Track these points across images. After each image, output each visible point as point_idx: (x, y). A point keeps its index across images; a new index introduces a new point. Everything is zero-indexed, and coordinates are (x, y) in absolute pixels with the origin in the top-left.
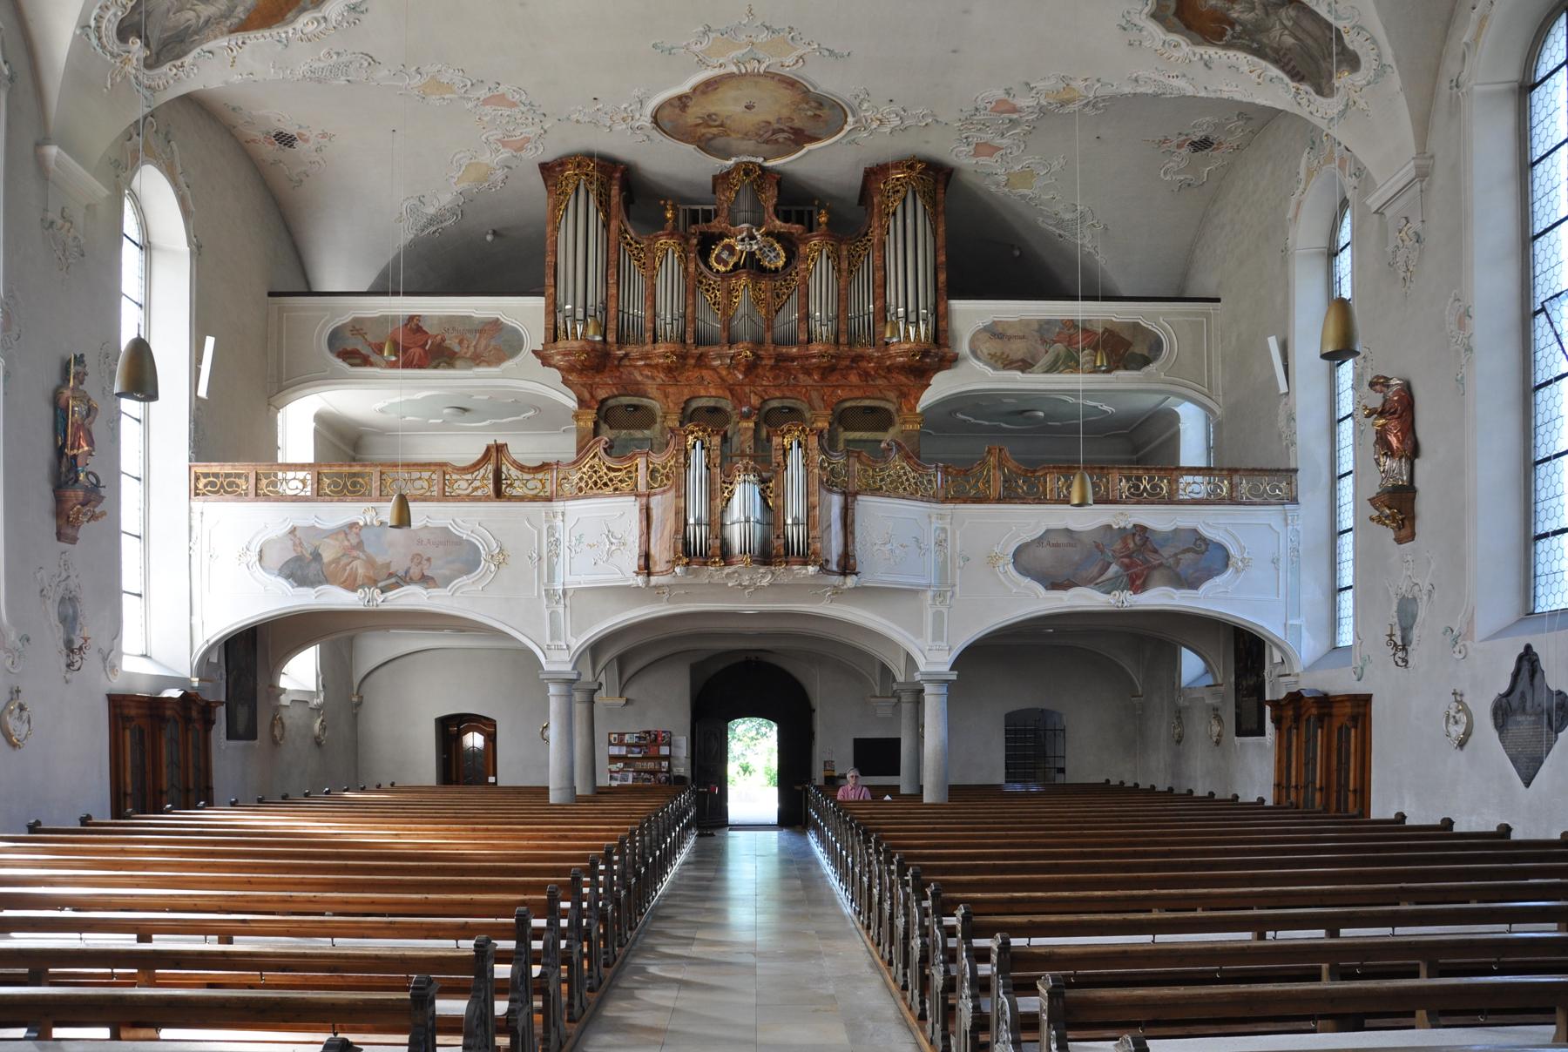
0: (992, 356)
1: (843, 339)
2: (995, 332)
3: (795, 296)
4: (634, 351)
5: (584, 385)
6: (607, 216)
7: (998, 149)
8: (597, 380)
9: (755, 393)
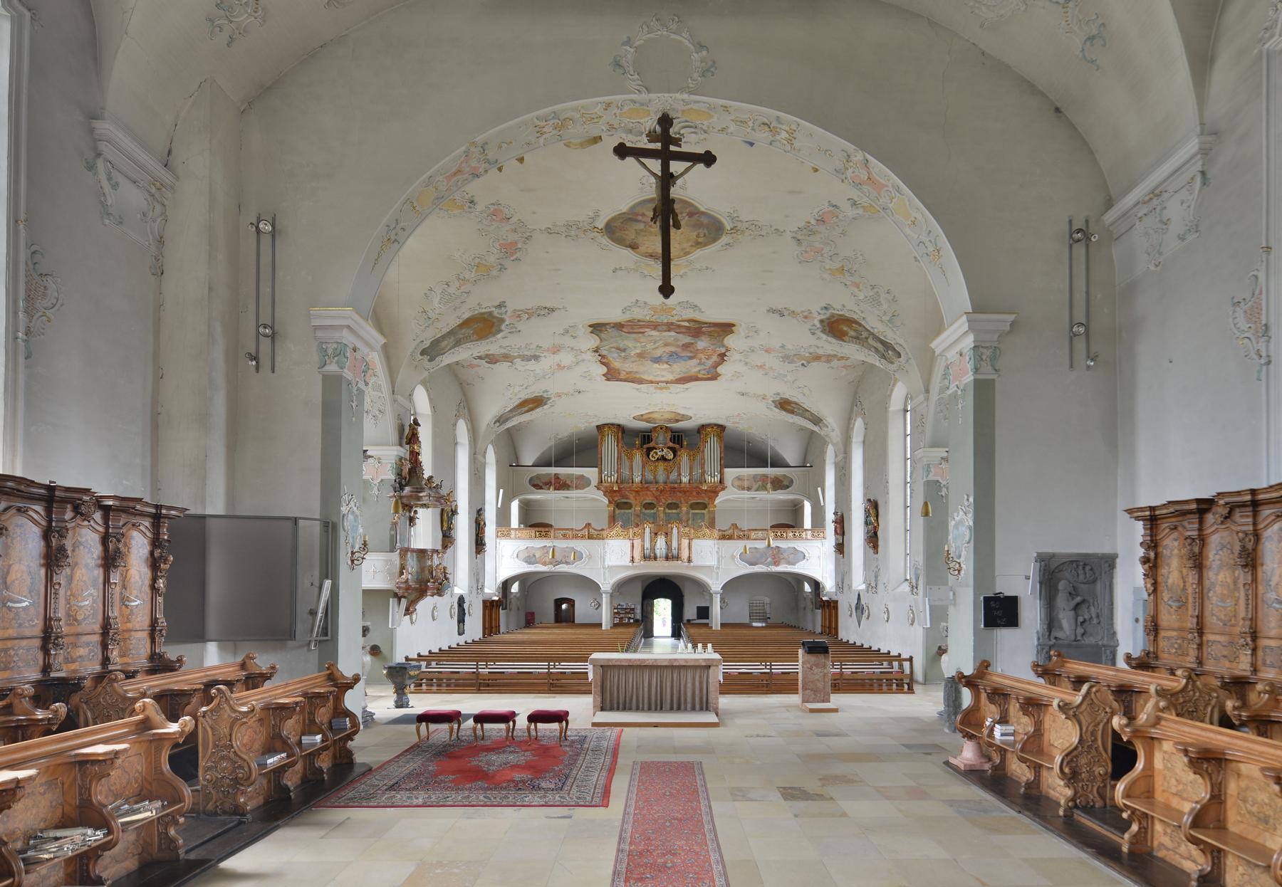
2: (739, 478)
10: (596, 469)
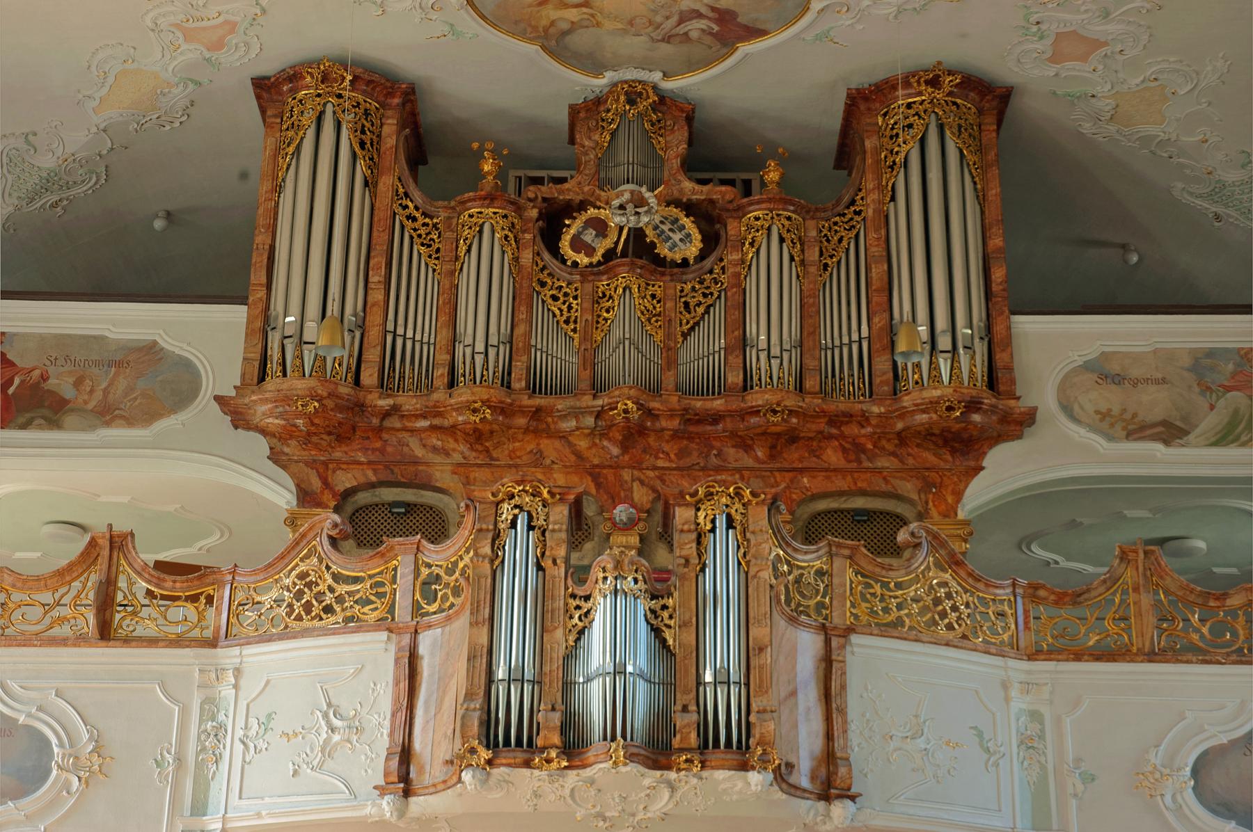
0: (1104, 415)
1: (811, 383)
3: (718, 311)
4: (409, 402)
5: (311, 464)
6: (373, 165)
7: (1097, 44)
8: (337, 454)
9: (642, 483)
10: (238, 313)
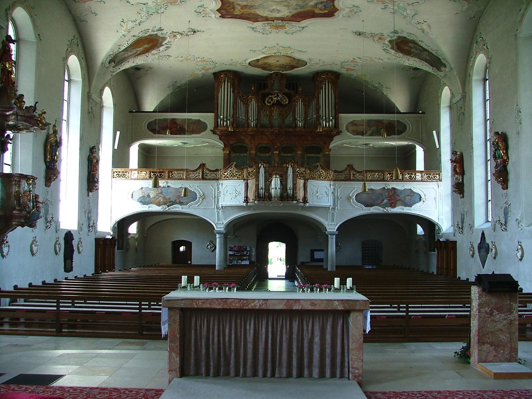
0: (353, 131)
1: (306, 126)
2: (353, 123)
